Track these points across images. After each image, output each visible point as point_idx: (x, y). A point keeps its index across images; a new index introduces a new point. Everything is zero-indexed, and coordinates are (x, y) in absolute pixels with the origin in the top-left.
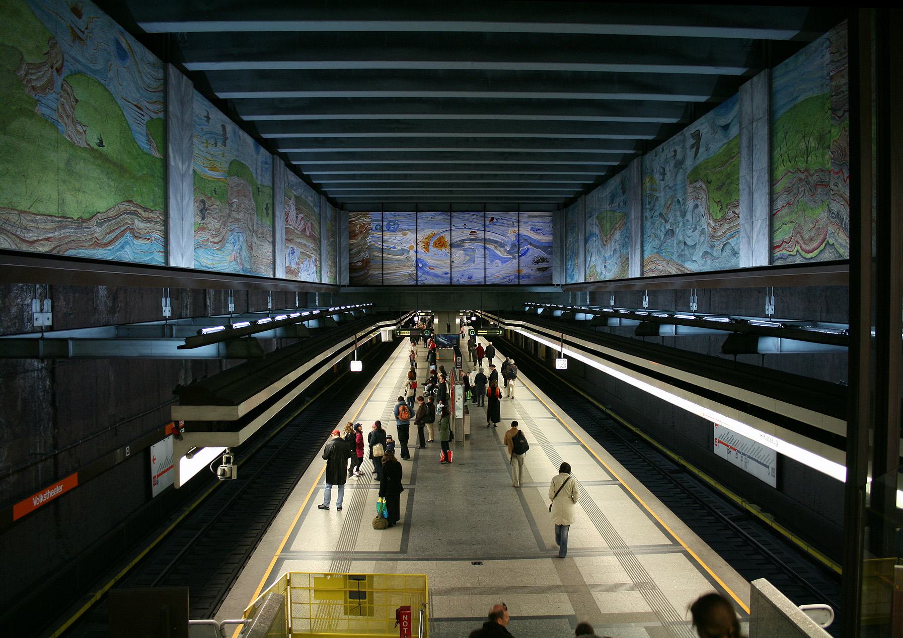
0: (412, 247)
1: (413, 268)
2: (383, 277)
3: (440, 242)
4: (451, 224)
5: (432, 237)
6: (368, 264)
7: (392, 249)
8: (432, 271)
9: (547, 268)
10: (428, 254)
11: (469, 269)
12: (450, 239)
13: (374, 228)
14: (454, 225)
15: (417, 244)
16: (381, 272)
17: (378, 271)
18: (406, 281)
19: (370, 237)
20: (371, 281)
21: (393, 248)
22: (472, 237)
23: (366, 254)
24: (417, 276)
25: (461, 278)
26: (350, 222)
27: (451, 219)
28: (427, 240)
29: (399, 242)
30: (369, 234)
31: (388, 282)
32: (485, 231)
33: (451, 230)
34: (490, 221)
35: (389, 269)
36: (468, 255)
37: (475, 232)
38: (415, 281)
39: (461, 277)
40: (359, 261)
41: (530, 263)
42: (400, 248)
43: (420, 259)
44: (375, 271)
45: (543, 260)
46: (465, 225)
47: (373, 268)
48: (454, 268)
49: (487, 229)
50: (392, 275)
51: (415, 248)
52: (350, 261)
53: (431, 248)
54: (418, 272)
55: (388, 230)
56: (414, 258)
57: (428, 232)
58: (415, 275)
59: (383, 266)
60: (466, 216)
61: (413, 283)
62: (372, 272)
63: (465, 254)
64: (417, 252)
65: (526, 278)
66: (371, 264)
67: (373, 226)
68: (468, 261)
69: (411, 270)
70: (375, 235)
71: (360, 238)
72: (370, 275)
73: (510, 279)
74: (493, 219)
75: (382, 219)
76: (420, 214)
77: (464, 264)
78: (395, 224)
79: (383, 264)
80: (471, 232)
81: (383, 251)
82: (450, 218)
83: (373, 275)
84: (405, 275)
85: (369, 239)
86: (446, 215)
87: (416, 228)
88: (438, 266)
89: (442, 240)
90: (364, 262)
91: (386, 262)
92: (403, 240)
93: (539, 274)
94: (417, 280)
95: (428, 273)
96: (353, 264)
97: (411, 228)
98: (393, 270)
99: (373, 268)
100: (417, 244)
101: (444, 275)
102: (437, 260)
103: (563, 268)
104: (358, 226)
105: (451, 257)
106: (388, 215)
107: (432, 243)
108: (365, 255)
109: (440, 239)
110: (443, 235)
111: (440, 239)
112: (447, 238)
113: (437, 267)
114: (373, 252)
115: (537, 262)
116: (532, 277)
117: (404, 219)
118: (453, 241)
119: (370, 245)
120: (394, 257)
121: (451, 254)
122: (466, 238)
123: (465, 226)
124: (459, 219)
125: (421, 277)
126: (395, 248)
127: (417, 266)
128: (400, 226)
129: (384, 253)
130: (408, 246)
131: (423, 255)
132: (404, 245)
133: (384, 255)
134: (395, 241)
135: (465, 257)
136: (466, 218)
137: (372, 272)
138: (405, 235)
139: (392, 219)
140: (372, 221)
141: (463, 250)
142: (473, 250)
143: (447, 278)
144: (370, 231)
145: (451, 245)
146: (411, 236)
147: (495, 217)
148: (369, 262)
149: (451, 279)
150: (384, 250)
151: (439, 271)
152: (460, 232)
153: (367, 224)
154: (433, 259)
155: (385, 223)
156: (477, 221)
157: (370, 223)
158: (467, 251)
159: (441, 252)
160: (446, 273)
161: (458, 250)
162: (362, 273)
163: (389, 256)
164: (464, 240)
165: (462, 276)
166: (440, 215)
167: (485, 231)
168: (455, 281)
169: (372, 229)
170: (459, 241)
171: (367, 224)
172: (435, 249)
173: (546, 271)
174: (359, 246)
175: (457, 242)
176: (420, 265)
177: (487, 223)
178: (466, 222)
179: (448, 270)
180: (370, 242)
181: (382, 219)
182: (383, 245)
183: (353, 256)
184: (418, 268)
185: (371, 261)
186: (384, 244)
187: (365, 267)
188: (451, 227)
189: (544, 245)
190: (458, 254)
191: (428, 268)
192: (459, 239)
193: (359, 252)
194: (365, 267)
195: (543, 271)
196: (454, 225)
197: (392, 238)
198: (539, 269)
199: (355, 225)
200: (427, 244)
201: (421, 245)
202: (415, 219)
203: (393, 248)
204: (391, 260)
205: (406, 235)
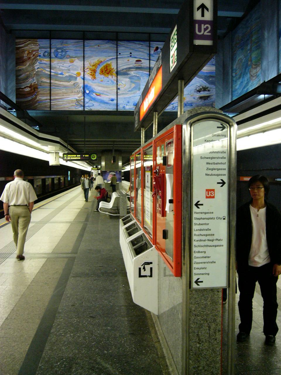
0: (79, 74)
1: (81, 94)
2: (50, 103)
3: (107, 70)
4: (117, 53)
5: (99, 65)
6: (36, 89)
7: (59, 76)
8: (99, 97)
9: (208, 97)
10: (95, 81)
11: (135, 96)
12: (116, 67)
13: (42, 55)
14: (120, 54)
15: (84, 71)
16: (49, 98)
17: (46, 96)
18: (73, 107)
19: (38, 64)
20: (40, 106)
21: (61, 74)
22: (137, 65)
23: (34, 80)
24: (84, 102)
25: (127, 105)
26: (18, 49)
27: (117, 48)
28: (94, 68)
29: (66, 68)
30: (38, 60)
31: (55, 107)
32: (150, 60)
33: (117, 58)
34: (155, 51)
35: (56, 94)
36: (134, 83)
37: (140, 61)
38: (83, 107)
39: (127, 103)
40: (27, 87)
41: (193, 92)
42: (67, 74)
43: (87, 86)
44: (43, 96)
45: (205, 89)
46: (131, 53)
47: (41, 94)
48: (120, 95)
49: (151, 58)
50: (60, 100)
51: (82, 75)
52: (16, 86)
53: (98, 75)
54: (85, 98)
55: (56, 57)
56: (81, 85)
57: (95, 60)
58: (83, 101)
59: (50, 92)
60: (132, 45)
61: (81, 109)
62: (38, 98)
63: (131, 82)
64: (84, 79)
65: (189, 105)
66: (39, 90)
67: (41, 52)
68: (133, 88)
69: (79, 96)
70: (43, 62)
71: (28, 64)
72: (38, 100)
73: (173, 106)
74: (157, 48)
75: (50, 46)
76: (87, 42)
77: (129, 91)
78: (62, 51)
79: (50, 90)
80: (137, 61)
81: (50, 77)
82: (116, 46)
83: (41, 101)
84: (72, 101)
85: (37, 65)
86: (112, 43)
87: (83, 55)
88: (105, 93)
89: (108, 68)
90: (33, 88)
91: (54, 88)
92: (71, 67)
93: (201, 102)
94: (84, 106)
95: (94, 99)
96: (21, 90)
97: (79, 55)
98: (61, 96)
99: (41, 94)
100: (84, 71)
101: (111, 102)
102: (104, 87)
103: (229, 91)
104: (26, 52)
105: (117, 84)
106: (56, 43)
107: (98, 71)
108: (32, 81)
109: (107, 67)
110: (109, 62)
111: (106, 67)
112: (113, 66)
113: (103, 94)
114: (41, 78)
115: (199, 91)
116: (194, 105)
117: (71, 46)
118: (119, 69)
119: (38, 71)
120: (61, 83)
121: (117, 82)
122: (131, 66)
123: (131, 55)
124: (124, 49)
125: (87, 103)
126: (63, 75)
127: (84, 92)
128: (68, 53)
129: (51, 79)
130: (76, 72)
131: (89, 82)
132: (72, 71)
133: (52, 81)
134: (63, 68)
135: (130, 85)
136: (131, 47)
137: (38, 98)
138: (72, 62)
139: (59, 46)
140: (40, 48)
141: (129, 78)
142: (139, 78)
143: (114, 104)
144: (38, 58)
145: (117, 73)
146: (78, 63)
147: (159, 46)
148: (37, 88)
149: (117, 106)
150: (52, 77)
151: (105, 98)
152: (126, 60)
153: (35, 51)
154: (99, 86)
155: (53, 50)
156: (142, 50)
157: (38, 50)
158: (133, 79)
159: (108, 79)
160: (112, 100)
161: (124, 78)
162: (30, 98)
163: (57, 82)
164: (130, 68)
165: (128, 102)
166: (106, 43)
167: (150, 60)
168: (120, 108)
169: (40, 56)
170: (125, 69)
171: (35, 51)
172: (102, 76)
173: (207, 99)
174: (27, 72)
175: (123, 70)
176: (87, 92)
177: (152, 52)
178: (131, 51)
179: (114, 97)
180: (38, 68)
181: (50, 46)
182: (50, 72)
183: (21, 82)
184: (86, 95)
185: (39, 87)
186: (52, 71)
187: (33, 92)
188: (117, 56)
189: (206, 75)
190: (124, 81)
191: (94, 94)
192: (125, 67)
193: (27, 78)
194: (33, 92)
195: (205, 99)
196: (120, 54)
197: (59, 64)
198: (201, 98)
199: (24, 51)
200: (94, 71)
201: (88, 72)
202: (83, 47)
203: (61, 74)
204: (58, 86)
205: (73, 62)
